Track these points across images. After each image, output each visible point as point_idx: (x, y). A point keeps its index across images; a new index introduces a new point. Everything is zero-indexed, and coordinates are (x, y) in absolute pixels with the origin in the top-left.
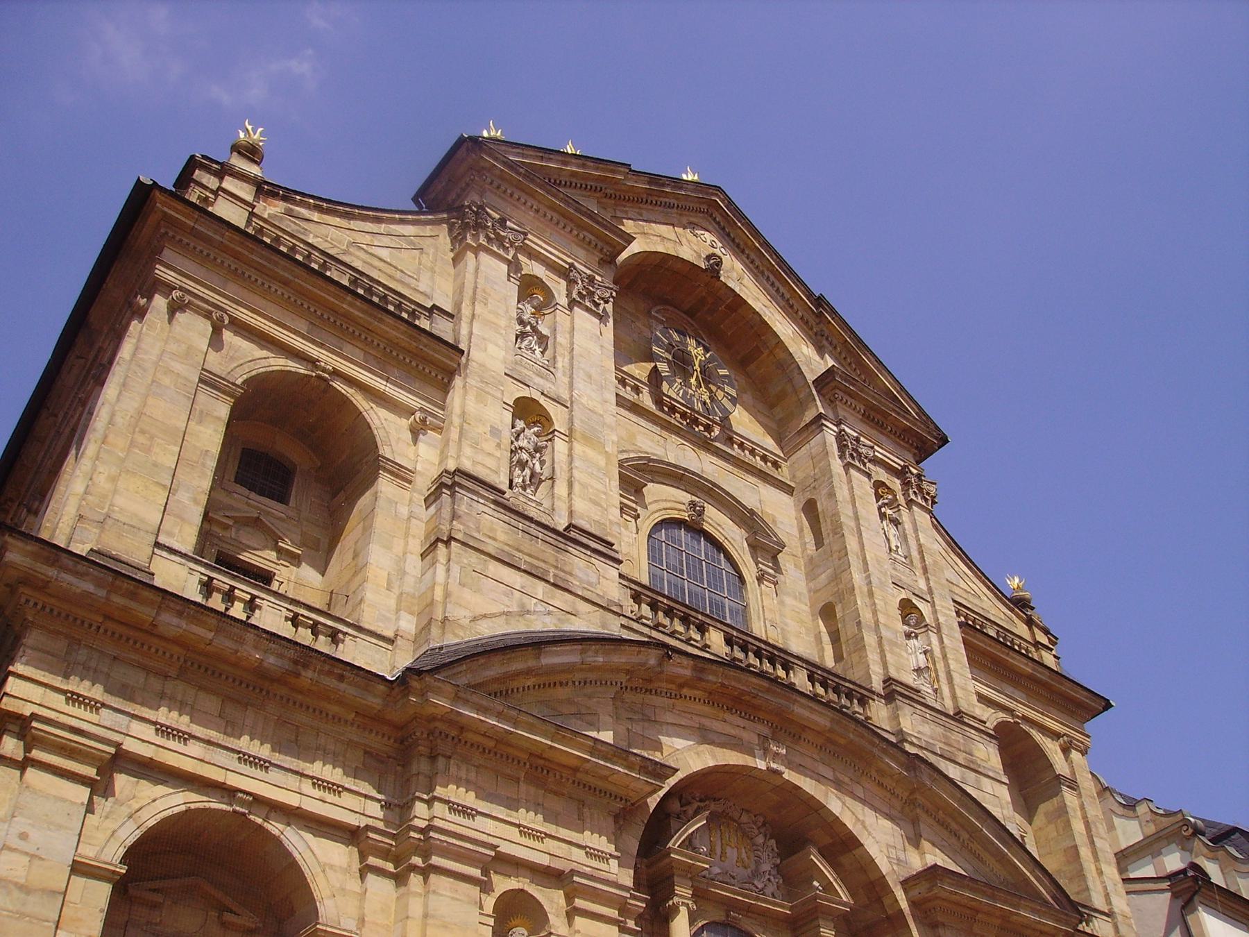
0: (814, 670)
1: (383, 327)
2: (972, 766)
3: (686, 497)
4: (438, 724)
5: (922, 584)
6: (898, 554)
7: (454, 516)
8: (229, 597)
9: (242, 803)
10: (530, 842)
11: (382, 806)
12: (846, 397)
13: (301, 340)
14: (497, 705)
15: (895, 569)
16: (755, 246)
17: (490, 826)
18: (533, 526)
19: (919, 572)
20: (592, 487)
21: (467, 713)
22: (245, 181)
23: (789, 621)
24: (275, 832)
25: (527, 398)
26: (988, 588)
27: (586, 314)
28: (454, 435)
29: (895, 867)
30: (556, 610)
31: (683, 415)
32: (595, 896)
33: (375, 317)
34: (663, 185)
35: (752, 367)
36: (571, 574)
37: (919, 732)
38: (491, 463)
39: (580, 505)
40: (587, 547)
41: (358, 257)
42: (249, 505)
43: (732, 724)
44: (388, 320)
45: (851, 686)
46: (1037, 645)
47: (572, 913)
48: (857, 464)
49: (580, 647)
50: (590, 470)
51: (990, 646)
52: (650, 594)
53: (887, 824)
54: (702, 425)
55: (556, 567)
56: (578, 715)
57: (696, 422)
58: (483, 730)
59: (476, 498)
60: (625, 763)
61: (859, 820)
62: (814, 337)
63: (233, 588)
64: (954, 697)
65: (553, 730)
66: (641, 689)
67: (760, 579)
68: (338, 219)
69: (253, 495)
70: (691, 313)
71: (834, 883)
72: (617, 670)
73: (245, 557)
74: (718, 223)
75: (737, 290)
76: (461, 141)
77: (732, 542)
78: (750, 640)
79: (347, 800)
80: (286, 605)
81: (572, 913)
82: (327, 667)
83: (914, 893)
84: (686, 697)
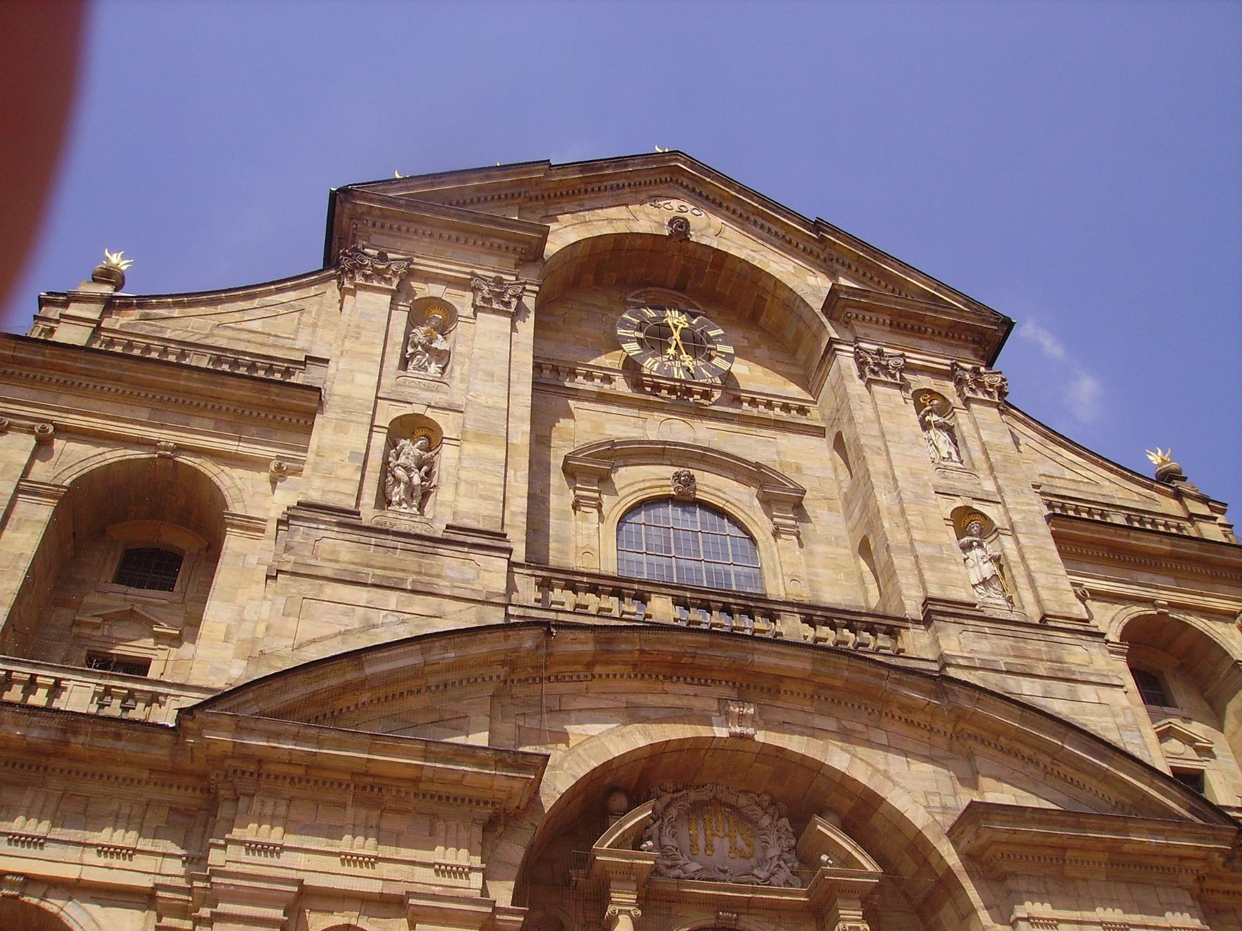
0: (812, 612)
1: (227, 390)
2: (1060, 675)
3: (669, 471)
4: (229, 762)
6: (952, 461)
10: (357, 870)
11: (184, 862)
12: (861, 314)
13: (138, 427)
14: (290, 726)
15: (945, 478)
16: (732, 195)
17: (301, 860)
18: (390, 537)
19: (983, 473)
20: (484, 483)
21: (253, 742)
22: (92, 302)
23: (820, 571)
24: (55, 909)
25: (410, 414)
26: (1111, 471)
27: (494, 316)
29: (938, 818)
30: (413, 616)
31: (672, 390)
33: (216, 384)
34: (601, 168)
35: (763, 319)
37: (972, 651)
41: (223, 337)
42: (125, 600)
43: (679, 694)
44: (230, 382)
45: (870, 619)
46: (1192, 518)
48: (883, 378)
49: (418, 647)
50: (483, 467)
51: (1098, 532)
52: (561, 576)
53: (927, 768)
54: (697, 393)
56: (440, 722)
57: (690, 392)
58: (286, 758)
59: (315, 526)
60: (474, 761)
61: (879, 771)
62: (824, 265)
63: (33, 676)
64: (1038, 601)
65: (368, 741)
66: (534, 679)
67: (776, 534)
68: (203, 308)
69: (132, 590)
70: (680, 287)
71: (854, 853)
72: (488, 664)
73: (120, 650)
74: (687, 187)
75: (715, 245)
76: (333, 196)
77: (737, 503)
78: (711, 597)
79: (140, 862)
80: (95, 681)
82: (99, 729)
84: (600, 676)
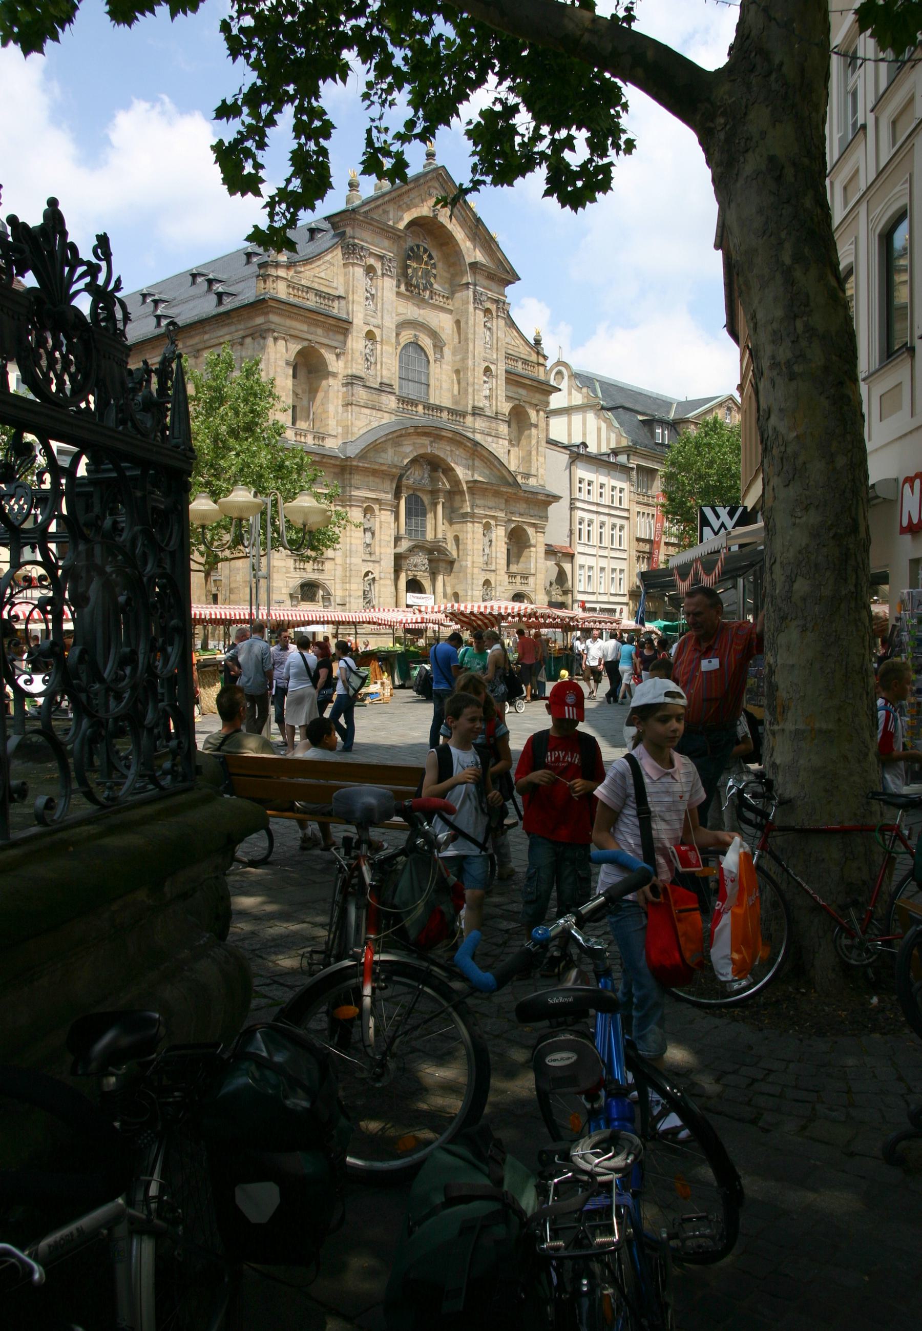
5: (495, 357)
7: (353, 395)
28: (350, 358)
32: (386, 504)
38: (360, 367)
39: (385, 373)
47: (380, 510)
64: (497, 406)
67: (435, 361)
81: (380, 510)
83: (469, 485)
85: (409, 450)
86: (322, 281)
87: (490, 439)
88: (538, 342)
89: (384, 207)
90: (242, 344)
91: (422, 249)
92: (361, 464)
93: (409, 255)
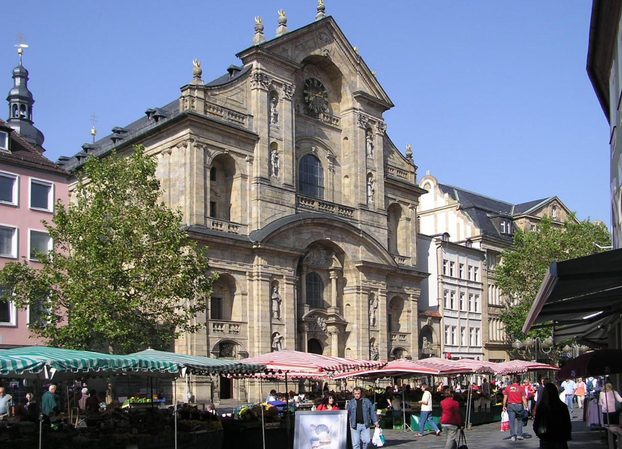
8: (217, 225)
9: (227, 271)
33: (237, 132)
36: (284, 200)
37: (366, 219)
40: (288, 190)
55: (281, 199)
74: (329, 30)
85: (308, 237)
86: (234, 103)
87: (373, 229)
88: (410, 156)
89: (284, 46)
90: (170, 153)
91: (316, 82)
92: (267, 248)
93: (305, 86)
